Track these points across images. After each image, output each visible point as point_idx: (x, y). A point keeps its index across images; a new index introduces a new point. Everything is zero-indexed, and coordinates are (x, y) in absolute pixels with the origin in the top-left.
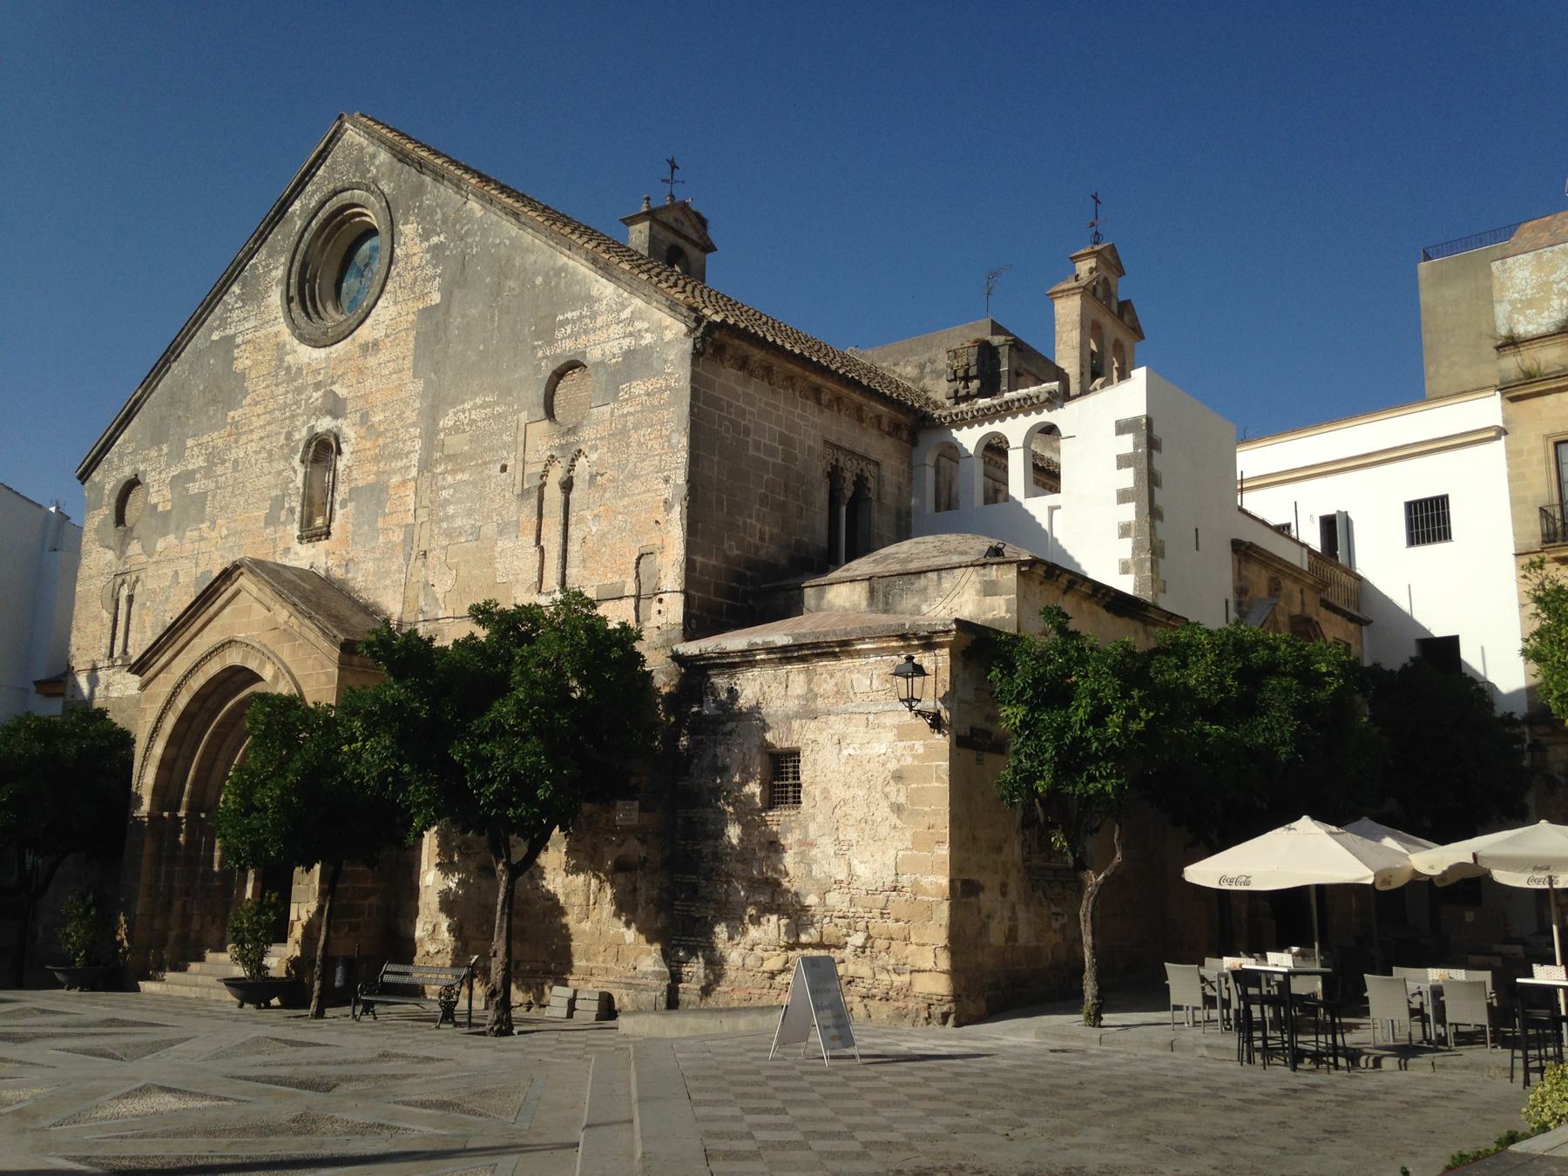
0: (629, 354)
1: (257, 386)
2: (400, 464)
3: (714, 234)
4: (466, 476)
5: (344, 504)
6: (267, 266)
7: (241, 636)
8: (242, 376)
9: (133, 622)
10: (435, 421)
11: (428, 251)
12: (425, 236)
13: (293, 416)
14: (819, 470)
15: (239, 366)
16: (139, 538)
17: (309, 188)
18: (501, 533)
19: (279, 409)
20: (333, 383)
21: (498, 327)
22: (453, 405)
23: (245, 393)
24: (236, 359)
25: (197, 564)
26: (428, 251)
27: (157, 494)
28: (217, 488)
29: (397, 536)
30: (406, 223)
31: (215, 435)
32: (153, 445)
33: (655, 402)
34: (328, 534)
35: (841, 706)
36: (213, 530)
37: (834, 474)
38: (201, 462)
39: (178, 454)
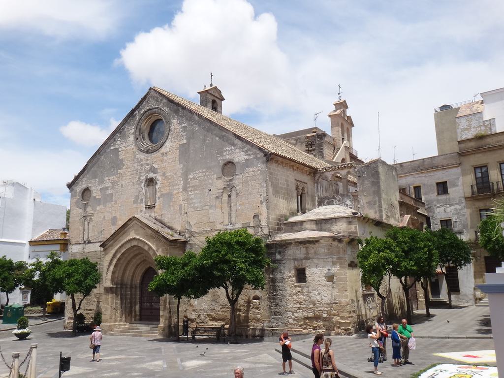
0: (246, 160)
1: (127, 163)
2: (177, 187)
3: (224, 94)
5: (159, 198)
6: (128, 129)
8: (122, 160)
9: (90, 231)
10: (187, 176)
12: (180, 124)
13: (140, 173)
14: (294, 188)
15: (121, 157)
17: (140, 107)
20: (153, 164)
21: (206, 150)
22: (192, 172)
23: (124, 165)
26: (181, 128)
27: (96, 193)
29: (177, 208)
33: (256, 174)
35: (316, 257)
37: (297, 188)
38: (110, 184)
39: (102, 182)
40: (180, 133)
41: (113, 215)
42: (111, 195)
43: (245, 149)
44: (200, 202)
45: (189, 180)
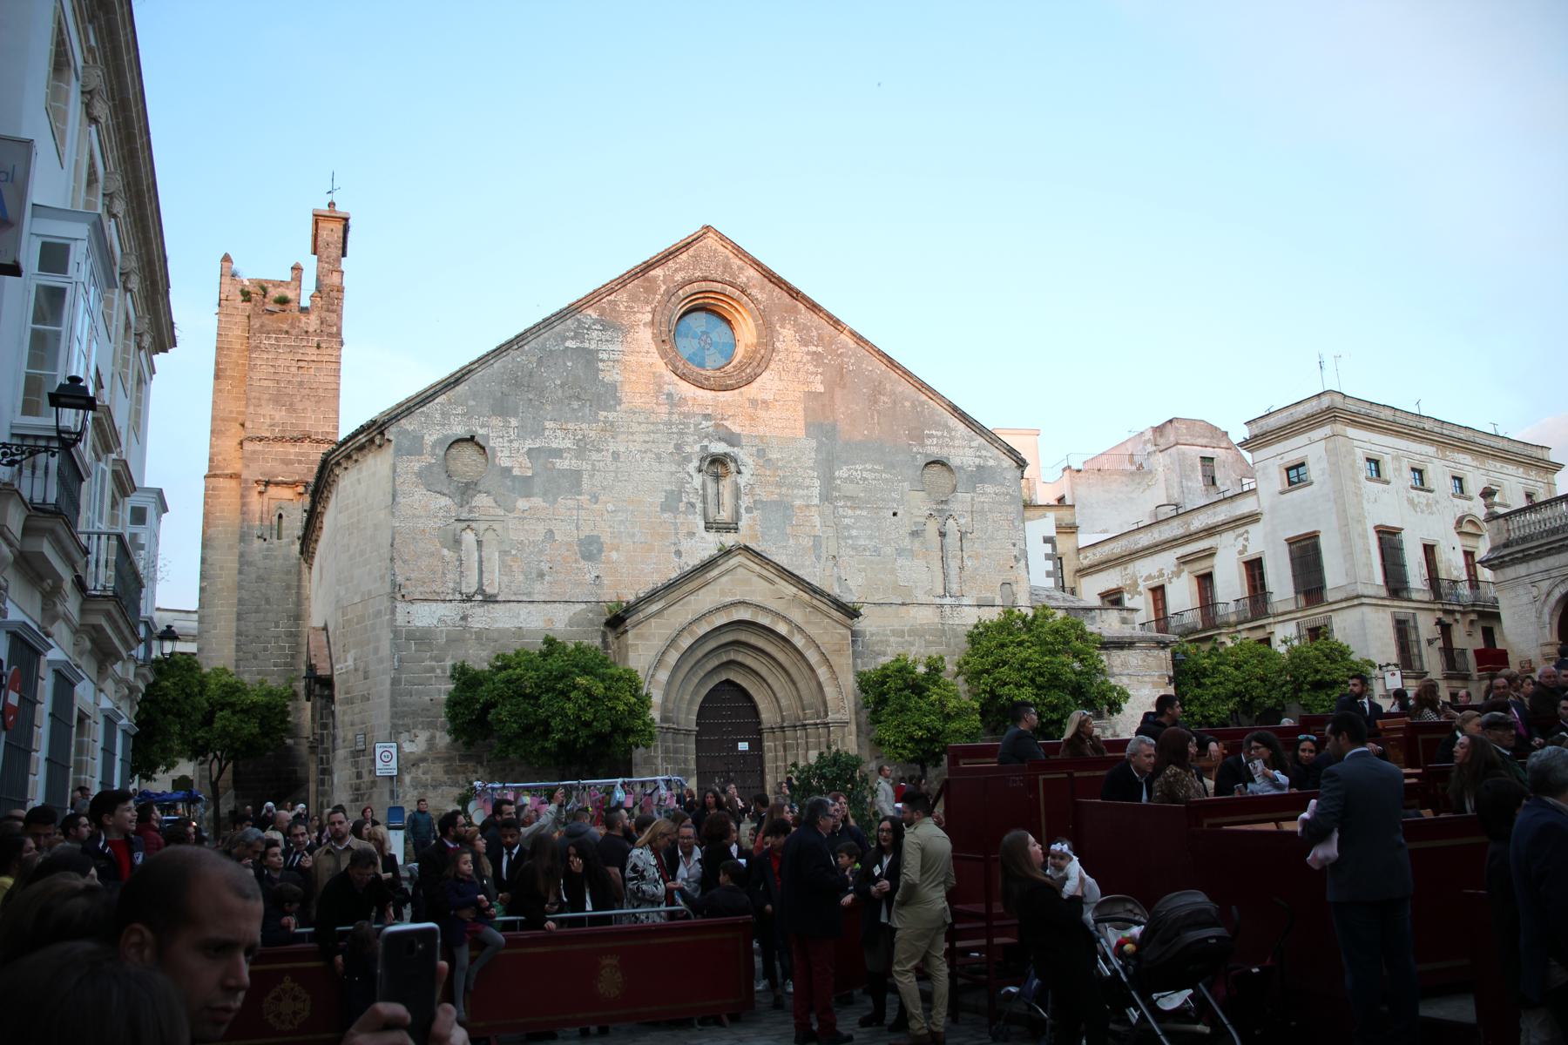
0: (979, 467)
4: (864, 513)
7: (747, 599)
8: (613, 387)
11: (808, 353)
13: (681, 433)
16: (488, 493)
18: (899, 554)
19: (665, 424)
22: (846, 463)
24: (602, 371)
25: (577, 529)
26: (808, 353)
28: (594, 470)
29: (807, 542)
30: (782, 327)
31: (584, 426)
32: (494, 414)
34: (736, 529)
35: (1126, 672)
36: (596, 503)
40: (804, 364)
41: (586, 531)
42: (576, 475)
43: (974, 444)
44: (871, 538)
45: (839, 482)
